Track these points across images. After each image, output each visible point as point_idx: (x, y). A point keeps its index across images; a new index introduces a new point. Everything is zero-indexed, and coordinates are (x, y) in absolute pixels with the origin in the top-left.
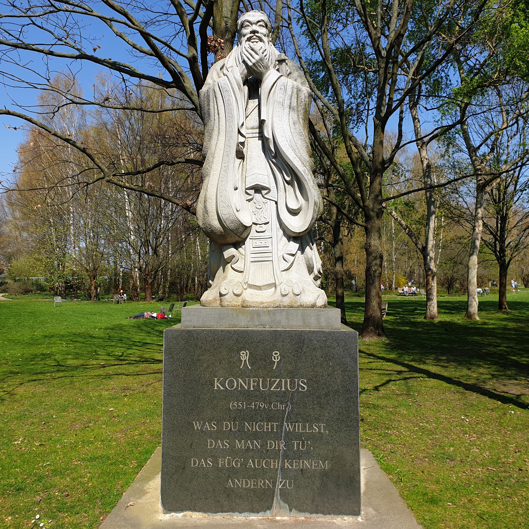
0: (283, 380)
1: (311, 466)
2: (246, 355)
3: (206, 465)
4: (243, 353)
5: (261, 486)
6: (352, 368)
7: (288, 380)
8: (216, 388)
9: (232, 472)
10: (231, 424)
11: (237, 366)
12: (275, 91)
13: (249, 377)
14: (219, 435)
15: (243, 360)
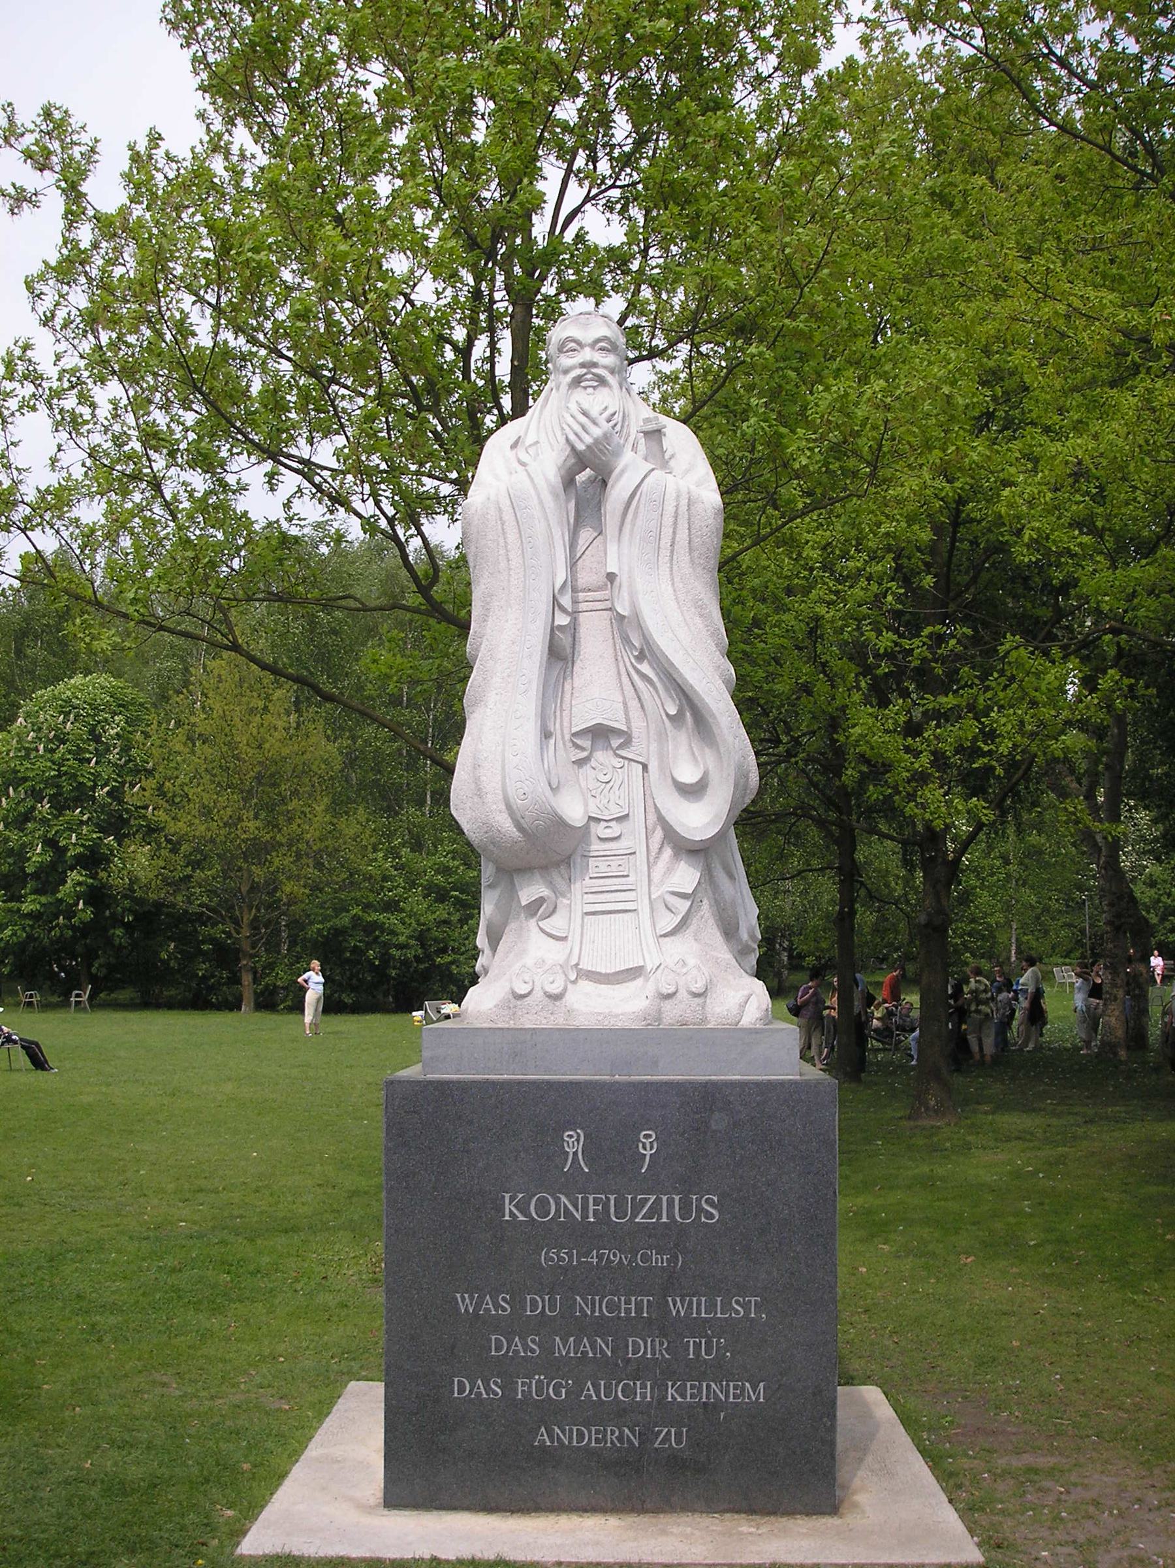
0: (664, 1198)
1: (727, 1397)
2: (578, 1141)
3: (488, 1394)
4: (570, 1136)
5: (612, 1442)
6: (824, 1165)
7: (677, 1198)
8: (507, 1218)
9: (549, 1413)
10: (543, 1301)
11: (557, 1167)
12: (637, 507)
13: (584, 1191)
14: (513, 1327)
15: (571, 1151)
